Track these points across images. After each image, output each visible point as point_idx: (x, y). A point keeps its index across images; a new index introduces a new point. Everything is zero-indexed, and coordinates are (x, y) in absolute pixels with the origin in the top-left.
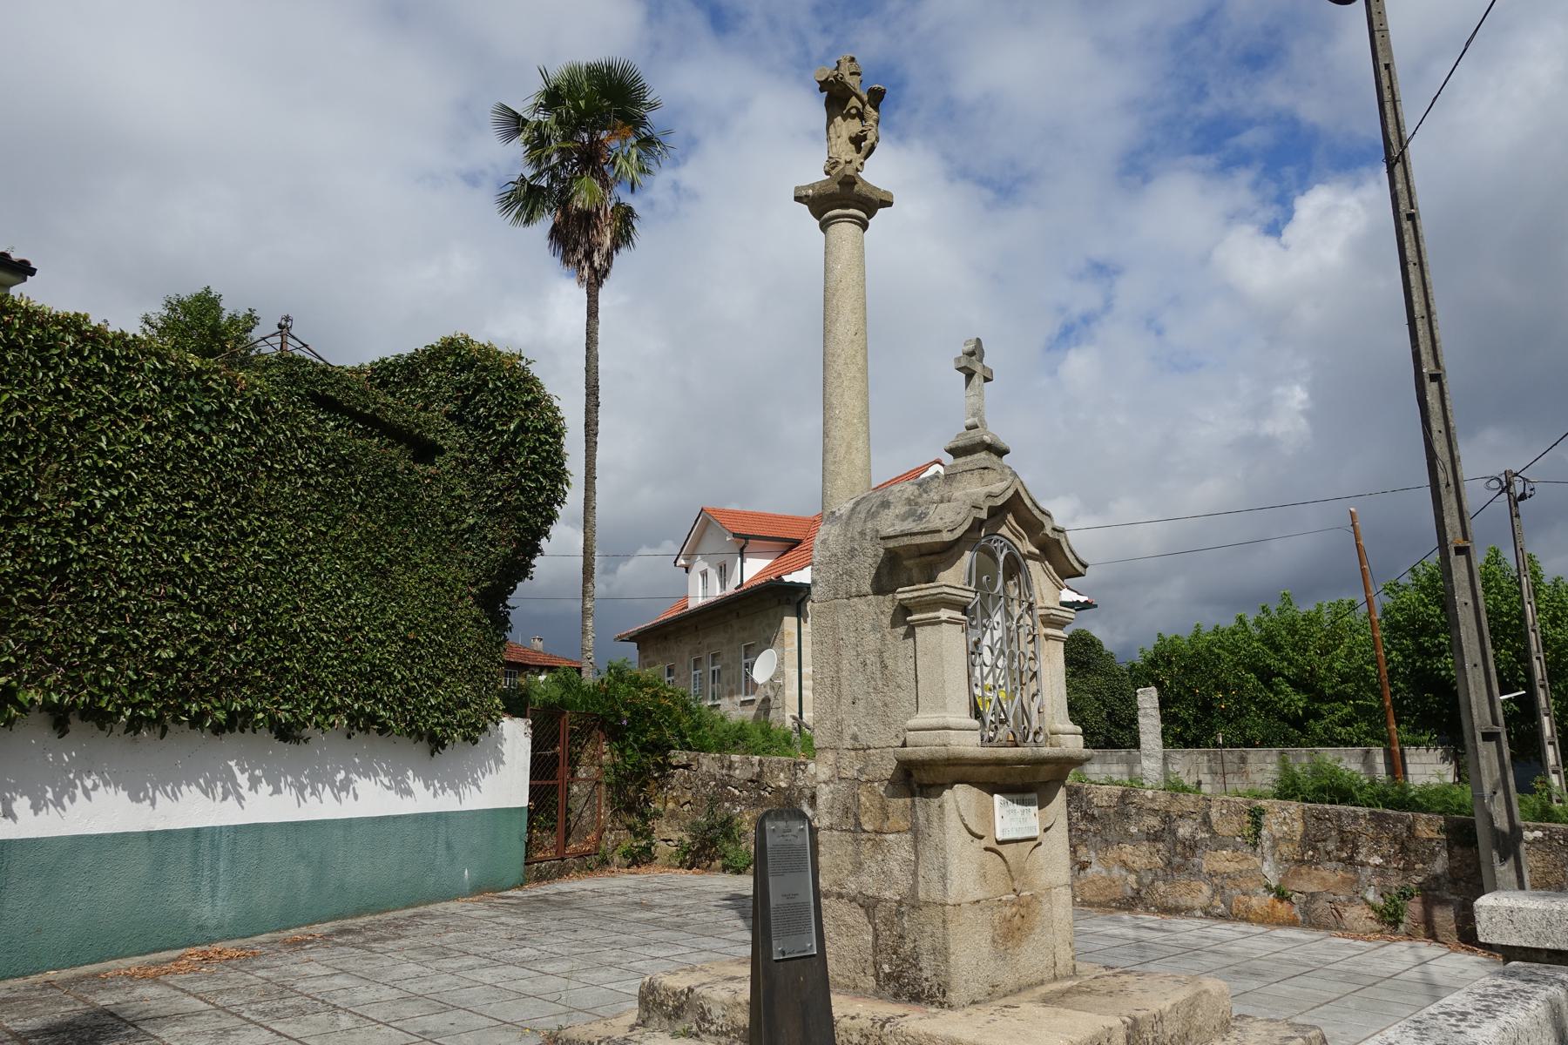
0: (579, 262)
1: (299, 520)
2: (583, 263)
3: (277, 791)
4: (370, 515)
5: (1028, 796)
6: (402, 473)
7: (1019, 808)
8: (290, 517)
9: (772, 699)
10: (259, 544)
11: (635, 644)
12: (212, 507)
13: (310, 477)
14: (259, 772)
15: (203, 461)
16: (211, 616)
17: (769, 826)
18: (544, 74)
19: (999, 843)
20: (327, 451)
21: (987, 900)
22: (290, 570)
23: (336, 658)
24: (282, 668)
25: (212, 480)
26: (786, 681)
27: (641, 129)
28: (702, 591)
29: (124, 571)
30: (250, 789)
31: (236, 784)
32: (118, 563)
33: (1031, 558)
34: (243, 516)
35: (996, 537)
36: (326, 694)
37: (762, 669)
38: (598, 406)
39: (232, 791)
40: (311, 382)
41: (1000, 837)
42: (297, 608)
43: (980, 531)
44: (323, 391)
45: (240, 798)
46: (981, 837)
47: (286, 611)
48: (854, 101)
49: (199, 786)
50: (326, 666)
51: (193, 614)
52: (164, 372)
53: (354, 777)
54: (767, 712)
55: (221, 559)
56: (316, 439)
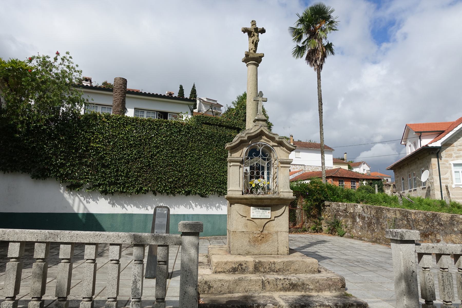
0: (314, 64)
1: (200, 151)
2: (315, 64)
3: (201, 207)
4: (219, 147)
5: (265, 208)
6: (228, 136)
7: (261, 211)
8: (198, 151)
9: (431, 187)
10: (190, 157)
11: (393, 171)
12: (179, 150)
13: (202, 141)
14: (197, 203)
15: (176, 141)
16: (180, 172)
17: (157, 209)
18: (298, 15)
19: (252, 218)
20: (206, 135)
22: (198, 161)
23: (211, 179)
24: (197, 182)
25: (178, 145)
26: (434, 181)
27: (330, 19)
28: (410, 150)
29: (161, 165)
30: (195, 207)
31: (192, 206)
32: (160, 163)
33: (275, 147)
34: (186, 151)
35: (258, 143)
36: (209, 187)
37: (424, 177)
38: (322, 104)
39: (191, 207)
40: (202, 120)
41: (252, 217)
42: (200, 169)
43: (249, 142)
44: (206, 122)
45: (193, 209)
46: (246, 217)
47: (197, 170)
48: (253, 33)
49: (184, 206)
50: (208, 181)
51: (176, 172)
52: (167, 125)
53: (221, 205)
54: (429, 192)
55: (182, 160)
56: (203, 133)
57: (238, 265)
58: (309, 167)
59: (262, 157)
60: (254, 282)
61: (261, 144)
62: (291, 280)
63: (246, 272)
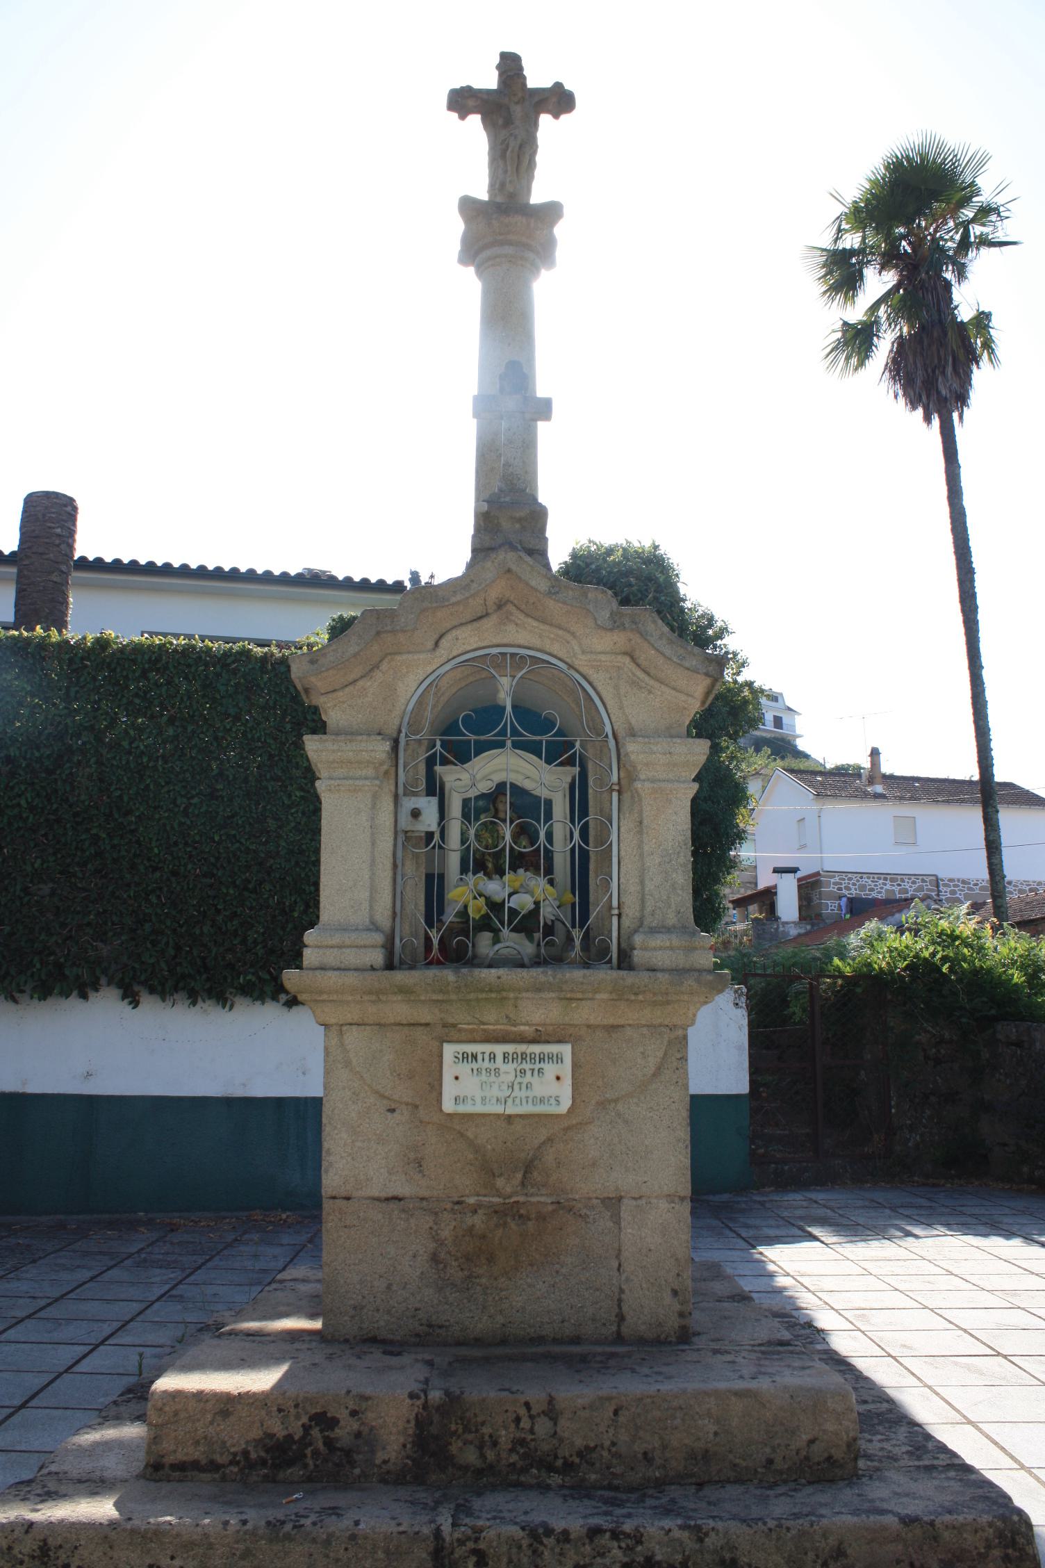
21: (422, 1199)
57: (305, 1419)
58: (955, 886)
59: (515, 732)
60: (380, 1555)
61: (513, 655)
62: (639, 1542)
63: (357, 1471)
